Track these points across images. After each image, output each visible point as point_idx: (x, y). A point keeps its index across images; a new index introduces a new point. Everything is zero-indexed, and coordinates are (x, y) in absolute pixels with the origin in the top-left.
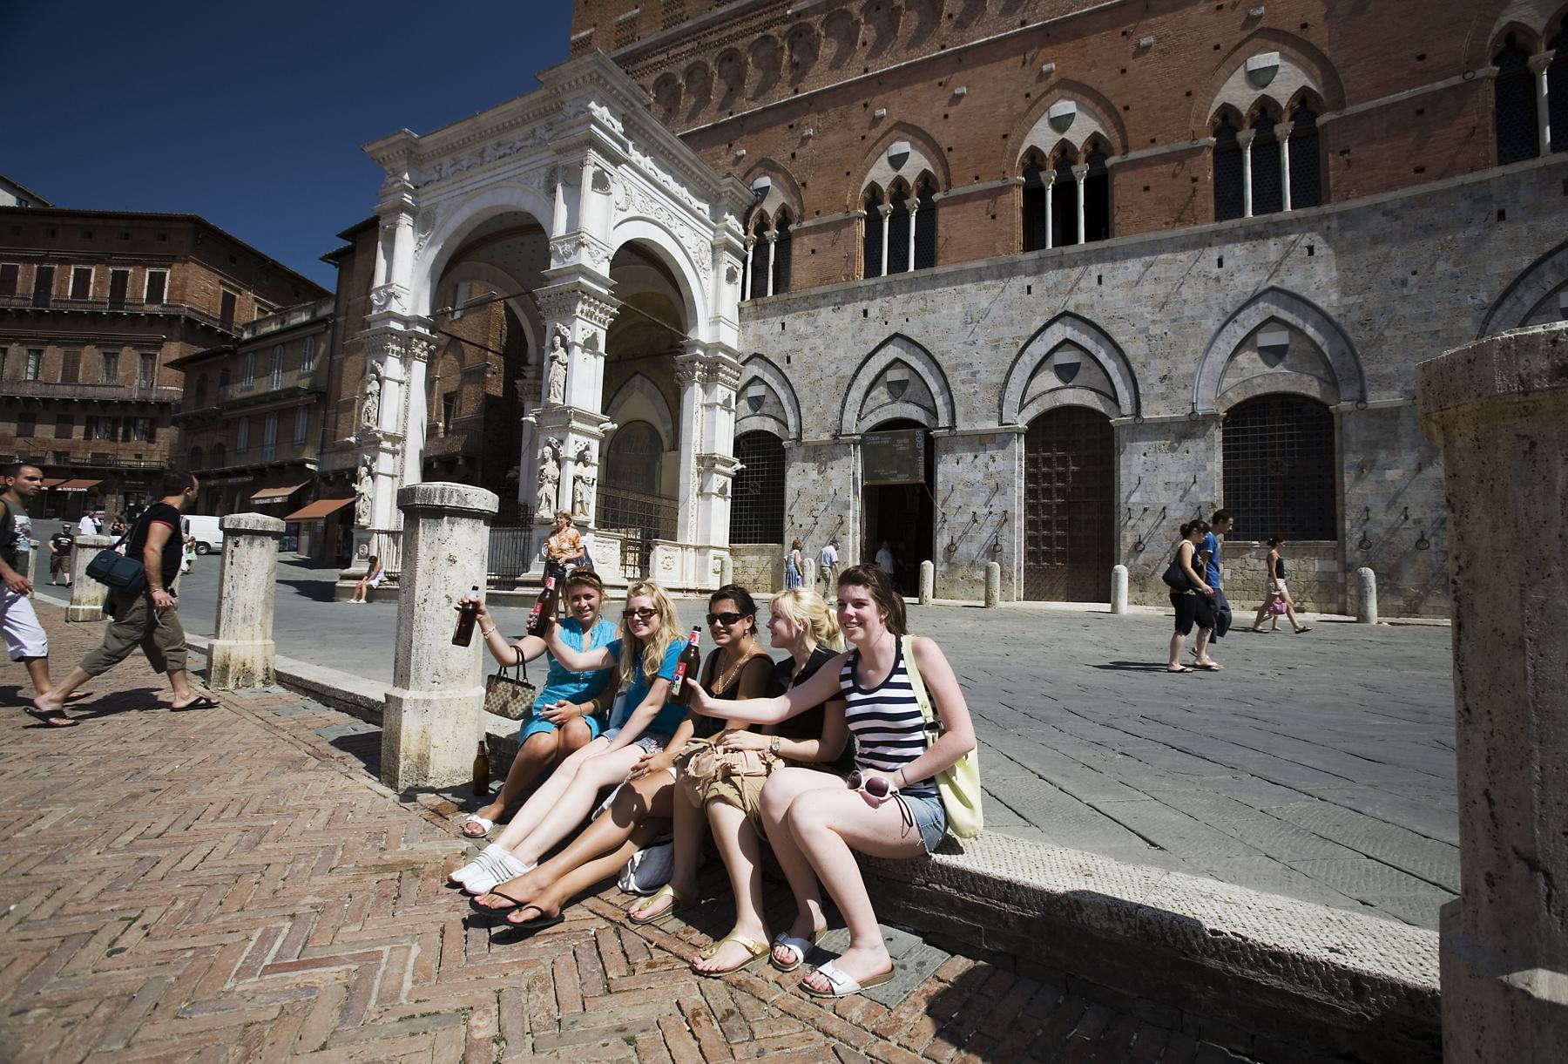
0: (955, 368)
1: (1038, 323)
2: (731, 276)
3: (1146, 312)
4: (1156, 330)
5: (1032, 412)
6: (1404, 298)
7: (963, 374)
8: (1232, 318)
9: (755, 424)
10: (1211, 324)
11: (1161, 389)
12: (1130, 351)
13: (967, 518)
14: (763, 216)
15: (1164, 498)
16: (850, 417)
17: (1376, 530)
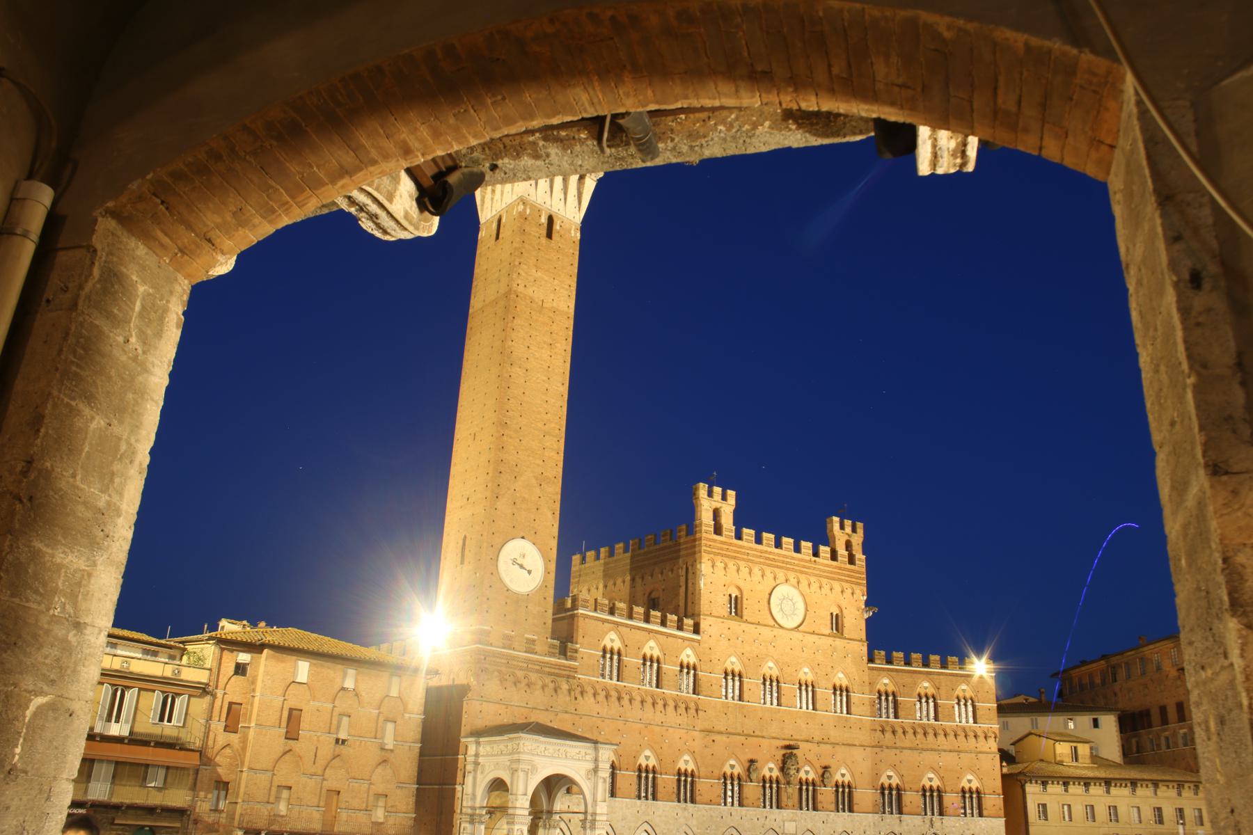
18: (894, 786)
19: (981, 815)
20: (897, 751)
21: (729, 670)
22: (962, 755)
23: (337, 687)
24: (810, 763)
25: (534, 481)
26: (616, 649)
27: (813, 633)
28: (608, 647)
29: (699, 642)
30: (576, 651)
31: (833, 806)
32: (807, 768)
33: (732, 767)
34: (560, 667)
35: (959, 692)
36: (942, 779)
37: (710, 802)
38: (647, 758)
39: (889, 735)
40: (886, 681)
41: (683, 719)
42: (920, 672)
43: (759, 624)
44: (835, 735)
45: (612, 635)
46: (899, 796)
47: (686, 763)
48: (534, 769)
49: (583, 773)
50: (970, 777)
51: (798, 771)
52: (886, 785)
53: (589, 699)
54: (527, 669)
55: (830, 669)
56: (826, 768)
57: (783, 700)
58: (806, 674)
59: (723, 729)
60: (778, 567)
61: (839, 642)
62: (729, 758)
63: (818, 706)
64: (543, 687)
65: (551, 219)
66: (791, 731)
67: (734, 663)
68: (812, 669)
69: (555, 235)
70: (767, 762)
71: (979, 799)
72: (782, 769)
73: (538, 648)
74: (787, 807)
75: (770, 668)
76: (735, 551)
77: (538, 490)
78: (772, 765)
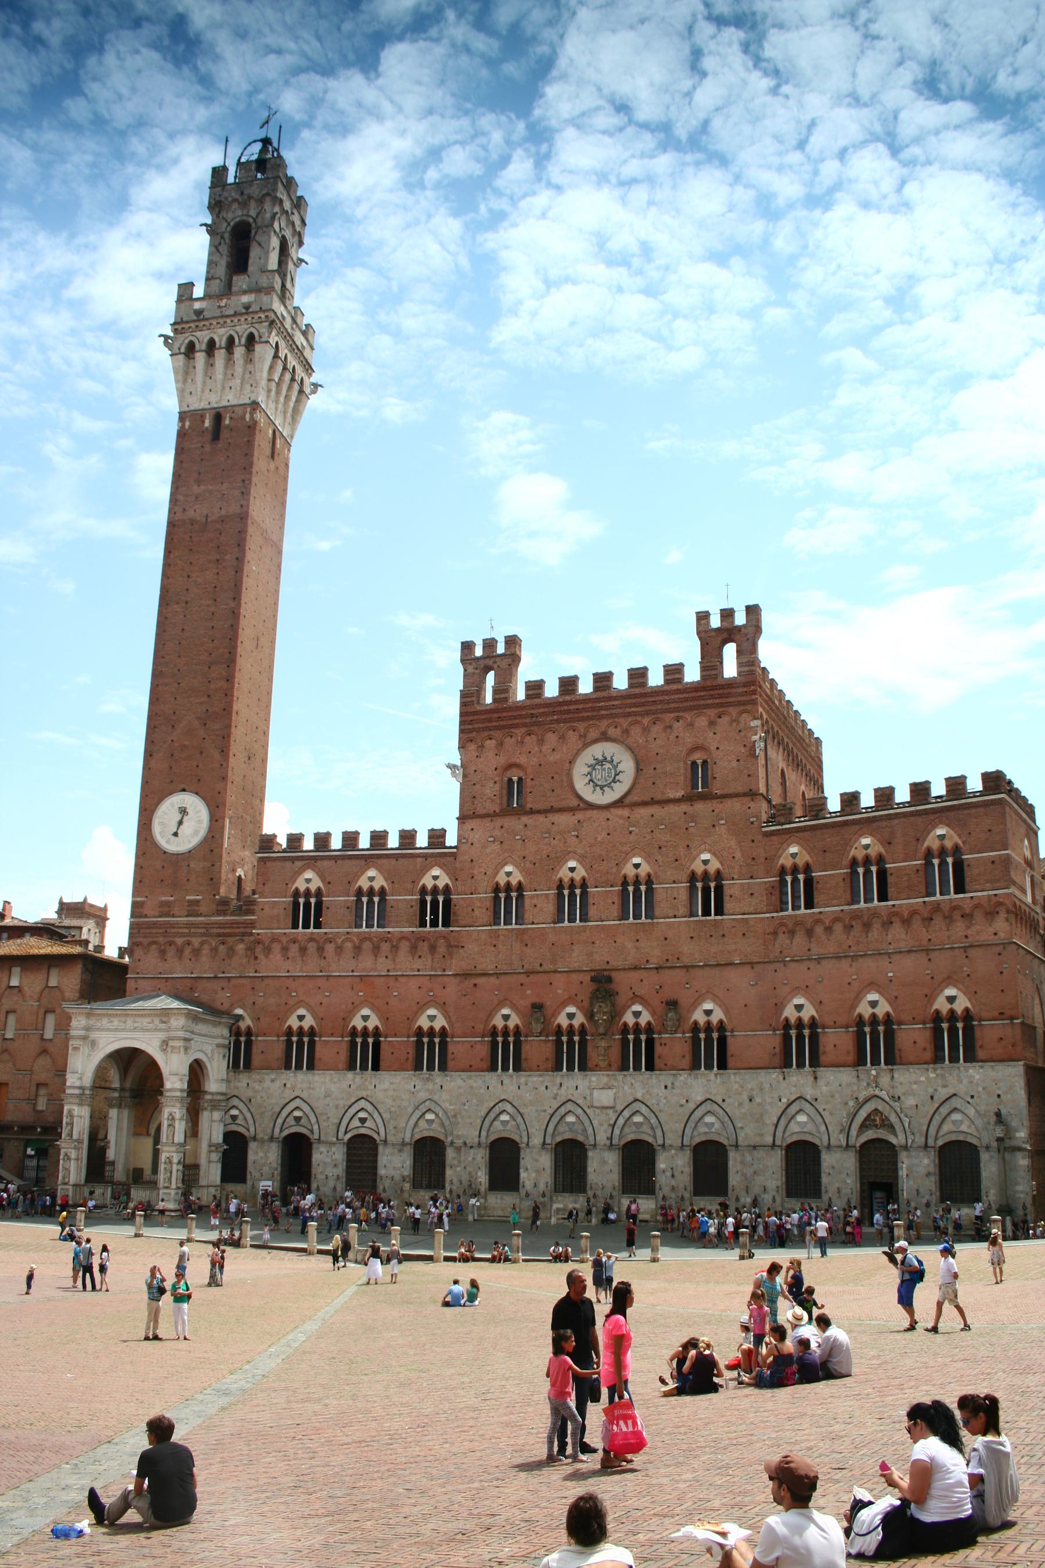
0: (322, 1114)
1: (353, 1100)
2: (224, 1056)
3: (390, 1102)
4: (393, 1109)
5: (349, 1136)
6: (465, 1110)
7: (324, 1118)
8: (417, 1108)
9: (234, 1128)
10: (410, 1110)
11: (393, 1132)
12: (384, 1116)
13: (324, 1177)
14: (239, 1028)
15: (392, 1173)
16: (277, 1130)
17: (454, 1188)
18: (806, 1019)
19: (971, 1057)
20: (811, 965)
21: (502, 883)
22: (934, 955)
23: (4, 986)
24: (636, 998)
25: (196, 723)
26: (313, 888)
27: (653, 802)
28: (302, 889)
29: (454, 855)
30: (253, 902)
31: (687, 1061)
32: (637, 1007)
33: (506, 1017)
34: (231, 924)
35: (932, 841)
36: (893, 1001)
37: (470, 1068)
38: (365, 1018)
39: (800, 939)
40: (794, 849)
41: (425, 964)
42: (854, 822)
43: (552, 810)
44: (691, 951)
45: (309, 874)
46: (814, 1038)
47: (432, 1018)
48: (94, 1043)
49: (157, 1043)
50: (951, 991)
51: (615, 1014)
52: (793, 1021)
53: (276, 956)
54: (189, 935)
55: (682, 851)
56: (672, 1004)
57: (592, 911)
58: (637, 865)
59: (490, 968)
60: (584, 719)
61: (700, 807)
62: (501, 1004)
63: (657, 912)
64: (214, 950)
65: (218, 418)
66: (602, 956)
67: (511, 873)
68: (647, 858)
69: (224, 434)
70: (564, 1004)
71: (969, 1030)
72: (585, 1015)
73: (203, 909)
74: (597, 1068)
75: (573, 868)
76: (510, 718)
77: (202, 733)
78: (571, 1009)
